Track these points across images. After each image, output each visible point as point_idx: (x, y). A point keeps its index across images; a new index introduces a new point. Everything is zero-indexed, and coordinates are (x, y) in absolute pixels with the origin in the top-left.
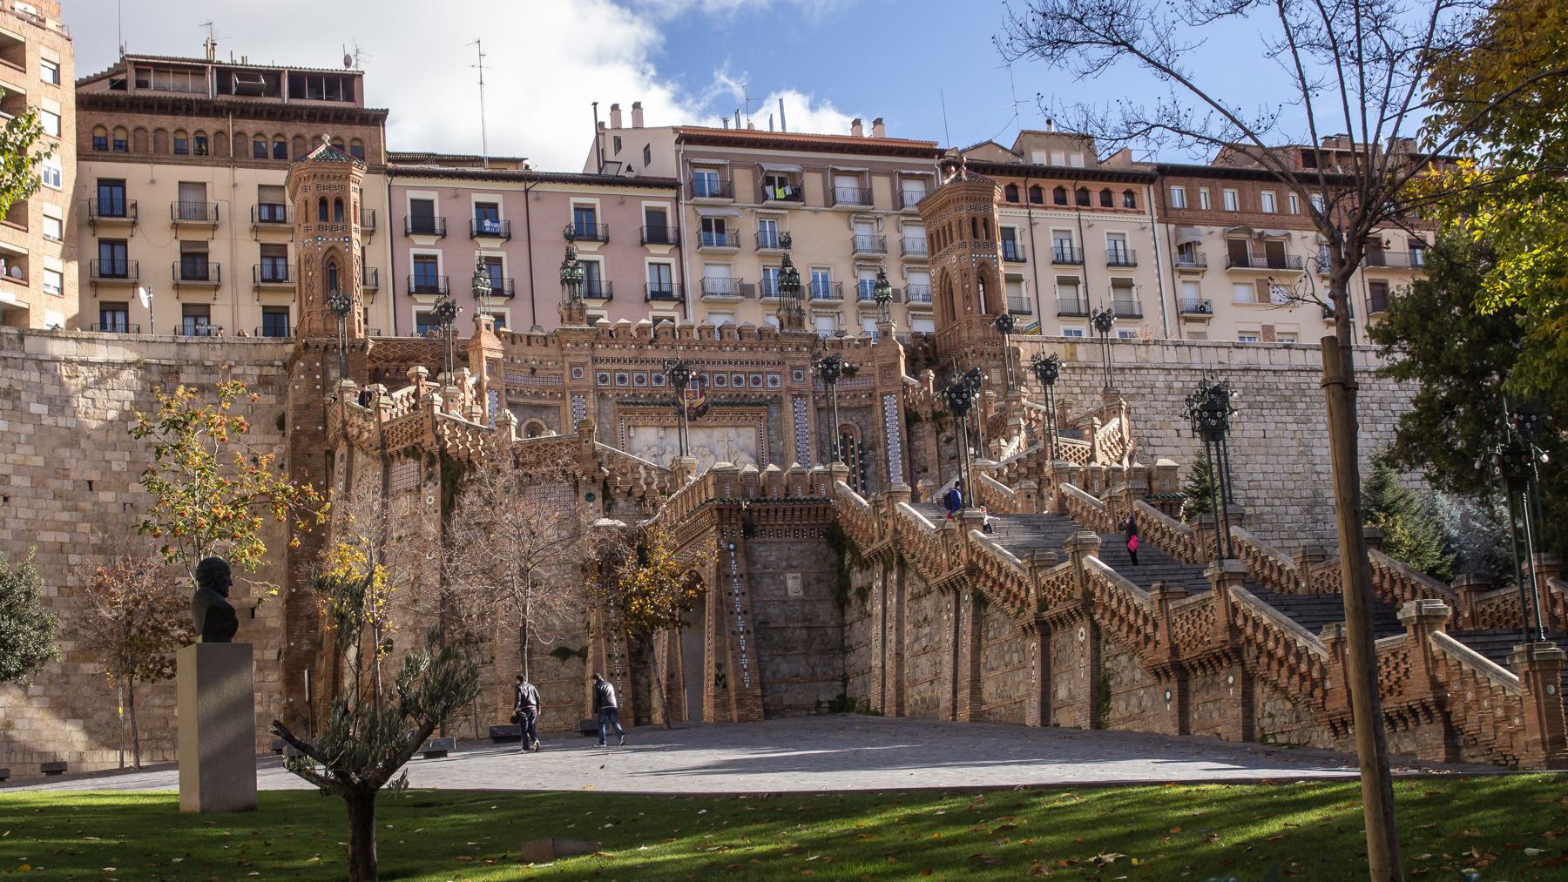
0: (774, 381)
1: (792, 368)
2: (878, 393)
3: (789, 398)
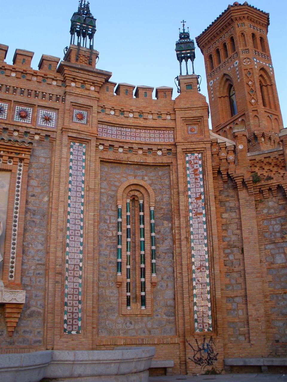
0: (47, 119)
1: (75, 105)
2: (179, 149)
3: (65, 140)
